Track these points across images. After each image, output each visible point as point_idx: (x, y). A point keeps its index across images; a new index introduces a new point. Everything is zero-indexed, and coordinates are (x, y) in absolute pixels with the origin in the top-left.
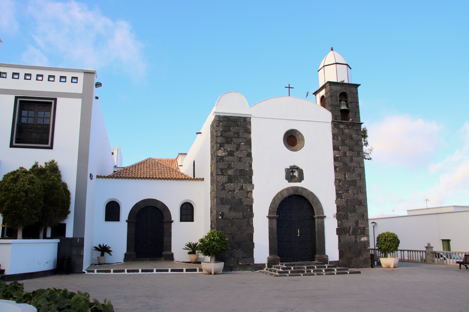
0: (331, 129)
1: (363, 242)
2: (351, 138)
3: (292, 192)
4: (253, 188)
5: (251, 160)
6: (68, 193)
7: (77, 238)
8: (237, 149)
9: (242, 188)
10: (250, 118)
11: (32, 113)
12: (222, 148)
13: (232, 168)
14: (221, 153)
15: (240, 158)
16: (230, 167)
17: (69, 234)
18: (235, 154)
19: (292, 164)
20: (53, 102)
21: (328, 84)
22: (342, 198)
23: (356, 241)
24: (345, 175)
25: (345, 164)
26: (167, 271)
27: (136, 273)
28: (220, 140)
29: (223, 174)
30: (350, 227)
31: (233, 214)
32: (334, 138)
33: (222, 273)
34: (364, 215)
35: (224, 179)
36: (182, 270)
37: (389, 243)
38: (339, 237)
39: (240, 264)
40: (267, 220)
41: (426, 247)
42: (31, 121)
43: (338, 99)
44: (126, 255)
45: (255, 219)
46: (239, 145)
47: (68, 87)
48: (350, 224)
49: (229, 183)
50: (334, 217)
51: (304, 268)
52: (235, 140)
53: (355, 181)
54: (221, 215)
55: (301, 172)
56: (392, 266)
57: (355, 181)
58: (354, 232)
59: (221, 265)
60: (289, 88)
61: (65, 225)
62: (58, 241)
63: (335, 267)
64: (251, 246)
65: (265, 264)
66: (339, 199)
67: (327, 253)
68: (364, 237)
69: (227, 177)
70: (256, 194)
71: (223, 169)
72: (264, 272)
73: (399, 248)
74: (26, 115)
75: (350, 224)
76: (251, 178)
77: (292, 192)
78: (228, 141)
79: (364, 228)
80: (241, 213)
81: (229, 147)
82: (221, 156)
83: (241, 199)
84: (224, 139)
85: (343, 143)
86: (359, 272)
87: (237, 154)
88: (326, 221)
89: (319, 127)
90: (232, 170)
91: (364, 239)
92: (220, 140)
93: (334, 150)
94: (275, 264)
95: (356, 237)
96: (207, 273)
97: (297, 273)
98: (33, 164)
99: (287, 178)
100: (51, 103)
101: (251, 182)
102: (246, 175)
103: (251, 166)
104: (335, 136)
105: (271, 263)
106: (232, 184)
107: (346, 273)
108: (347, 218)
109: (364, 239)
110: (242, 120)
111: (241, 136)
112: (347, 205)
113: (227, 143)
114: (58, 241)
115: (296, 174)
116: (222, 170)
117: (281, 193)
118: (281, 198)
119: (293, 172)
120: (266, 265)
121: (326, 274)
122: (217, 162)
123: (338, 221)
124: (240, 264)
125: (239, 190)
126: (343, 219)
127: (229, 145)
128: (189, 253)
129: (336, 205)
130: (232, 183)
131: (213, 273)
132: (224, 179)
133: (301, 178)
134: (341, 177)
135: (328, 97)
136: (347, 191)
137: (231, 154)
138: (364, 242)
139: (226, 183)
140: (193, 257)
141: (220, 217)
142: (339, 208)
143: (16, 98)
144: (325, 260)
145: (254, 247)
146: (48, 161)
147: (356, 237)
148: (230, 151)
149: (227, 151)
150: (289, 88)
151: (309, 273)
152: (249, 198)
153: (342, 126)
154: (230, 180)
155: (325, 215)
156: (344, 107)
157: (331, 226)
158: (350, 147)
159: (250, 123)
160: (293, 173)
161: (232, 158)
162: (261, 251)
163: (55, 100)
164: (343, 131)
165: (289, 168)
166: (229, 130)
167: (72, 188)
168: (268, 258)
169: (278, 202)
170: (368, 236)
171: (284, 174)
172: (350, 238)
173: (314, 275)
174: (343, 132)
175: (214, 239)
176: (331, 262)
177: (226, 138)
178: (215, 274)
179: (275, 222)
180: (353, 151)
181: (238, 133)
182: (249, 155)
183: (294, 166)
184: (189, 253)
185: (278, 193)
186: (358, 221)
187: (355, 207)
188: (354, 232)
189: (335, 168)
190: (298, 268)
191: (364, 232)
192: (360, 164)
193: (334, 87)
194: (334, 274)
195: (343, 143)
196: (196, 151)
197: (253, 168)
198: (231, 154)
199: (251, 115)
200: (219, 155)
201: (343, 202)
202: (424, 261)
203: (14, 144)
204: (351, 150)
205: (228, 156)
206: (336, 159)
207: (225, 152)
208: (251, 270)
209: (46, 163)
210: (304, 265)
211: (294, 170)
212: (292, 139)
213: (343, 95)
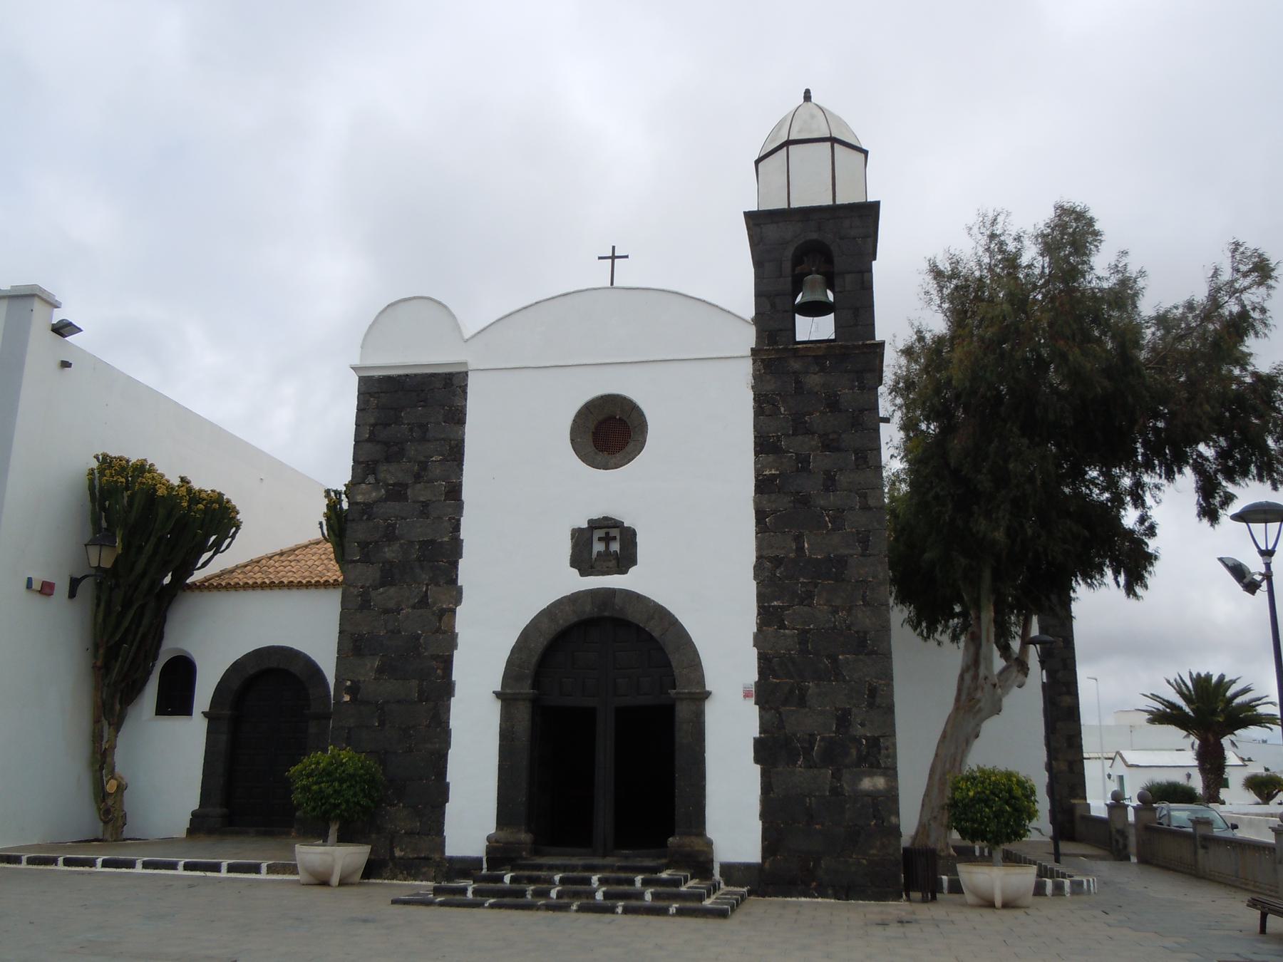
1: (868, 794)
2: (833, 404)
3: (588, 608)
4: (458, 599)
8: (418, 478)
9: (423, 602)
10: (466, 373)
12: (371, 479)
13: (397, 539)
15: (425, 505)
16: (390, 536)
18: (409, 492)
23: (836, 791)
24: (798, 539)
25: (803, 501)
27: (124, 870)
30: (812, 735)
32: (759, 411)
33: (360, 884)
35: (370, 573)
40: (496, 706)
44: (195, 816)
46: (424, 466)
49: (382, 585)
50: (747, 695)
52: (411, 450)
53: (842, 562)
54: (349, 690)
55: (629, 537)
58: (833, 755)
64: (439, 793)
65: (479, 860)
66: (770, 630)
67: (712, 831)
70: (466, 621)
76: (455, 565)
77: (589, 610)
79: (874, 742)
81: (391, 473)
83: (418, 637)
85: (799, 426)
87: (419, 493)
90: (396, 546)
95: (837, 775)
96: (312, 880)
99: (574, 563)
101: (453, 581)
102: (442, 556)
103: (457, 527)
106: (392, 590)
108: (802, 702)
113: (388, 460)
117: (549, 613)
123: (761, 709)
124: (398, 853)
125: (414, 607)
129: (755, 650)
130: (392, 584)
131: (335, 880)
132: (370, 573)
133: (625, 560)
137: (397, 493)
138: (873, 795)
139: (376, 588)
145: (447, 800)
147: (837, 775)
148: (394, 485)
152: (445, 632)
154: (389, 576)
155: (708, 688)
159: (465, 393)
162: (471, 816)
164: (798, 382)
165: (585, 525)
169: (539, 644)
170: (891, 772)
171: (565, 548)
176: (728, 869)
179: (523, 713)
180: (838, 449)
181: (423, 427)
182: (454, 493)
183: (606, 518)
187: (834, 660)
192: (864, 496)
195: (799, 426)
197: (464, 534)
198: (397, 493)
199: (465, 364)
204: (829, 445)
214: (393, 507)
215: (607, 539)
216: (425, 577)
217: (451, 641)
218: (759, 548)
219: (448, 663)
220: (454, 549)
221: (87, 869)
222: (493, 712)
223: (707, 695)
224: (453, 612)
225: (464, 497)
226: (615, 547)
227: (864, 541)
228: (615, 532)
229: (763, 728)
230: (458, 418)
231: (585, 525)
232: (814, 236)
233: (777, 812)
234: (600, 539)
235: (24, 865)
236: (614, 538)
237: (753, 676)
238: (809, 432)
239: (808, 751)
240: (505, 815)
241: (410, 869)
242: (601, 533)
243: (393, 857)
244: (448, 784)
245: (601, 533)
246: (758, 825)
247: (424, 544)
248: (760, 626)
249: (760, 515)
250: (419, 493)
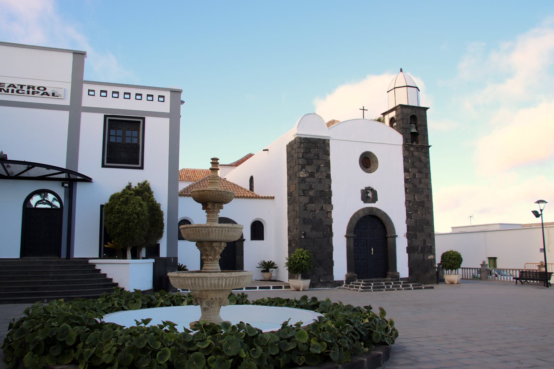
0: (402, 152)
2: (421, 161)
3: (367, 212)
4: (332, 209)
5: (330, 181)
6: (161, 214)
7: (171, 258)
8: (318, 171)
9: (322, 209)
11: (120, 132)
12: (304, 170)
13: (313, 189)
14: (302, 174)
15: (320, 179)
16: (311, 188)
17: (163, 253)
19: (367, 186)
21: (399, 107)
22: (411, 219)
23: (424, 259)
24: (414, 196)
25: (415, 186)
26: (255, 288)
28: (301, 161)
29: (304, 195)
30: (418, 246)
32: (404, 161)
34: (431, 235)
35: (305, 200)
36: (269, 288)
37: (452, 260)
38: (409, 256)
39: (321, 281)
40: (345, 239)
41: (482, 265)
42: (119, 140)
43: (409, 122)
45: (334, 238)
46: (319, 167)
47: (156, 106)
48: (418, 243)
51: (382, 284)
52: (315, 162)
53: (423, 202)
54: (303, 235)
55: (375, 193)
56: (456, 282)
57: (423, 202)
59: (307, 282)
60: (363, 110)
61: (159, 245)
62: (153, 260)
63: (410, 283)
65: (343, 281)
66: (409, 219)
67: (398, 271)
69: (308, 197)
71: (305, 190)
72: (343, 288)
73: (462, 266)
74: (114, 134)
75: (418, 243)
76: (330, 198)
77: (367, 213)
78: (309, 162)
79: (431, 247)
80: (322, 233)
81: (310, 169)
86: (433, 288)
88: (397, 240)
89: (390, 148)
90: (313, 191)
91: (430, 257)
92: (301, 161)
94: (353, 281)
95: (423, 256)
97: (378, 288)
98: (128, 184)
100: (140, 122)
101: (330, 203)
102: (325, 196)
103: (330, 187)
104: (405, 159)
105: (349, 280)
106: (313, 205)
107: (422, 288)
108: (416, 238)
109: (430, 257)
110: (322, 142)
112: (416, 225)
113: (308, 164)
114: (153, 260)
115: (370, 195)
116: (303, 191)
117: (357, 213)
119: (367, 193)
120: (345, 282)
121: (414, 289)
122: (299, 183)
124: (321, 281)
127: (310, 167)
128: (263, 271)
129: (406, 225)
130: (313, 203)
132: (305, 200)
133: (374, 199)
135: (399, 120)
136: (416, 211)
138: (430, 260)
139: (308, 204)
140: (267, 275)
143: (105, 116)
144: (396, 277)
145: (333, 265)
146: (141, 181)
149: (309, 172)
150: (363, 110)
151: (388, 289)
153: (412, 149)
156: (414, 130)
157: (401, 244)
159: (329, 145)
160: (369, 195)
161: (312, 179)
163: (144, 119)
166: (310, 152)
167: (164, 208)
168: (346, 276)
169: (355, 222)
172: (418, 256)
173: (394, 290)
174: (413, 155)
175: (303, 258)
176: (402, 279)
177: (307, 159)
178: (303, 290)
179: (352, 241)
181: (318, 155)
182: (329, 176)
184: (263, 271)
185: (355, 213)
186: (425, 240)
187: (422, 227)
188: (423, 251)
189: (406, 189)
190: (378, 284)
191: (431, 250)
192: (428, 186)
193: (405, 110)
194: (411, 289)
195: (413, 166)
196: (272, 172)
197: (332, 189)
198: (312, 175)
200: (301, 176)
202: (474, 278)
203: (106, 164)
204: (420, 172)
205: (309, 177)
206: (406, 181)
207: (306, 173)
208: (331, 287)
209: (139, 184)
210: (381, 281)
211: (368, 191)
213: (413, 118)
219: (331, 227)
220: (330, 194)
222: (344, 241)
224: (331, 212)
230: (328, 154)
232: (414, 114)
235: (283, 289)
237: (406, 232)
238: (416, 168)
240: (349, 269)
243: (320, 282)
244: (333, 262)
247: (321, 191)
248: (407, 218)
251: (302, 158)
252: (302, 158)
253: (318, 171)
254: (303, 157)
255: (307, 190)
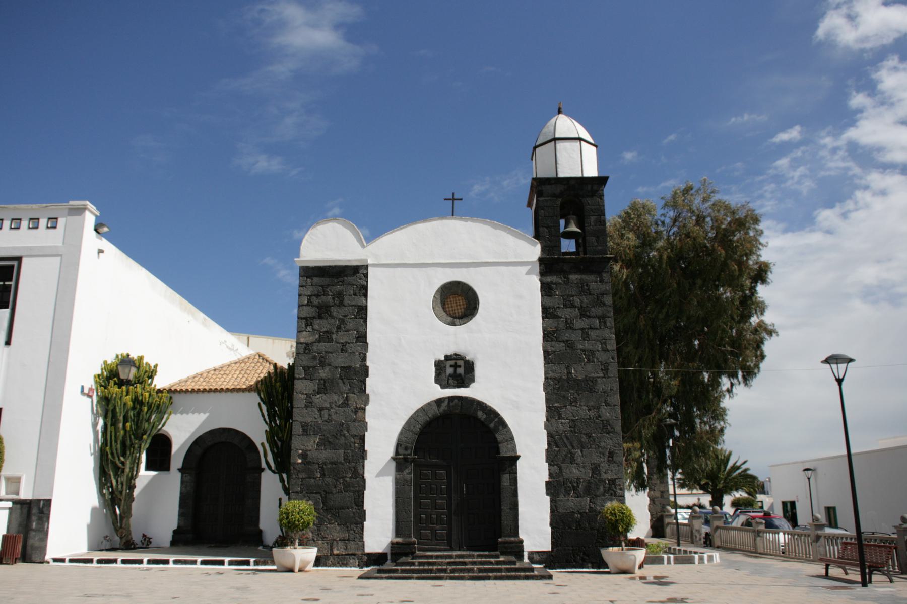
4: (367, 402)
9: (346, 403)
10: (366, 267)
15: (344, 345)
20: (15, 263)
25: (570, 345)
28: (308, 311)
31: (325, 455)
46: (342, 321)
49: (318, 393)
52: (335, 311)
53: (594, 381)
55: (469, 367)
58: (589, 491)
68: (611, 500)
70: (372, 414)
71: (309, 368)
78: (323, 311)
80: (342, 452)
81: (322, 325)
82: (307, 344)
84: (314, 309)
90: (327, 369)
92: (308, 311)
93: (543, 318)
99: (438, 380)
101: (363, 390)
102: (358, 375)
103: (364, 359)
108: (572, 461)
111: (346, 302)
118: (423, 419)
120: (389, 557)
123: (550, 465)
124: (335, 552)
126: (564, 461)
129: (545, 432)
134: (560, 371)
137: (326, 337)
141: (300, 461)
142: (553, 440)
144: (517, 549)
145: (365, 520)
148: (324, 332)
150: (453, 199)
155: (518, 454)
158: (581, 308)
172: (571, 502)
182: (362, 337)
183: (456, 355)
185: (417, 411)
201: (563, 426)
204: (584, 313)
205: (320, 342)
212: (458, 302)
214: (323, 346)
215: (455, 366)
216: (345, 388)
217: (364, 426)
218: (546, 373)
219: (362, 439)
220: (365, 372)
221: (137, 566)
223: (518, 457)
224: (364, 410)
225: (368, 341)
226: (461, 371)
227: (606, 370)
228: (461, 363)
229: (550, 475)
230: (363, 291)
231: (443, 359)
233: (560, 523)
234: (451, 366)
236: (460, 367)
238: (573, 306)
239: (575, 489)
240: (399, 529)
241: (342, 561)
242: (452, 363)
244: (365, 511)
245: (452, 363)
246: (549, 529)
249: (546, 353)
250: (342, 337)
251: (308, 305)
252: (308, 305)
253: (339, 328)
254: (310, 304)
255: (314, 367)
